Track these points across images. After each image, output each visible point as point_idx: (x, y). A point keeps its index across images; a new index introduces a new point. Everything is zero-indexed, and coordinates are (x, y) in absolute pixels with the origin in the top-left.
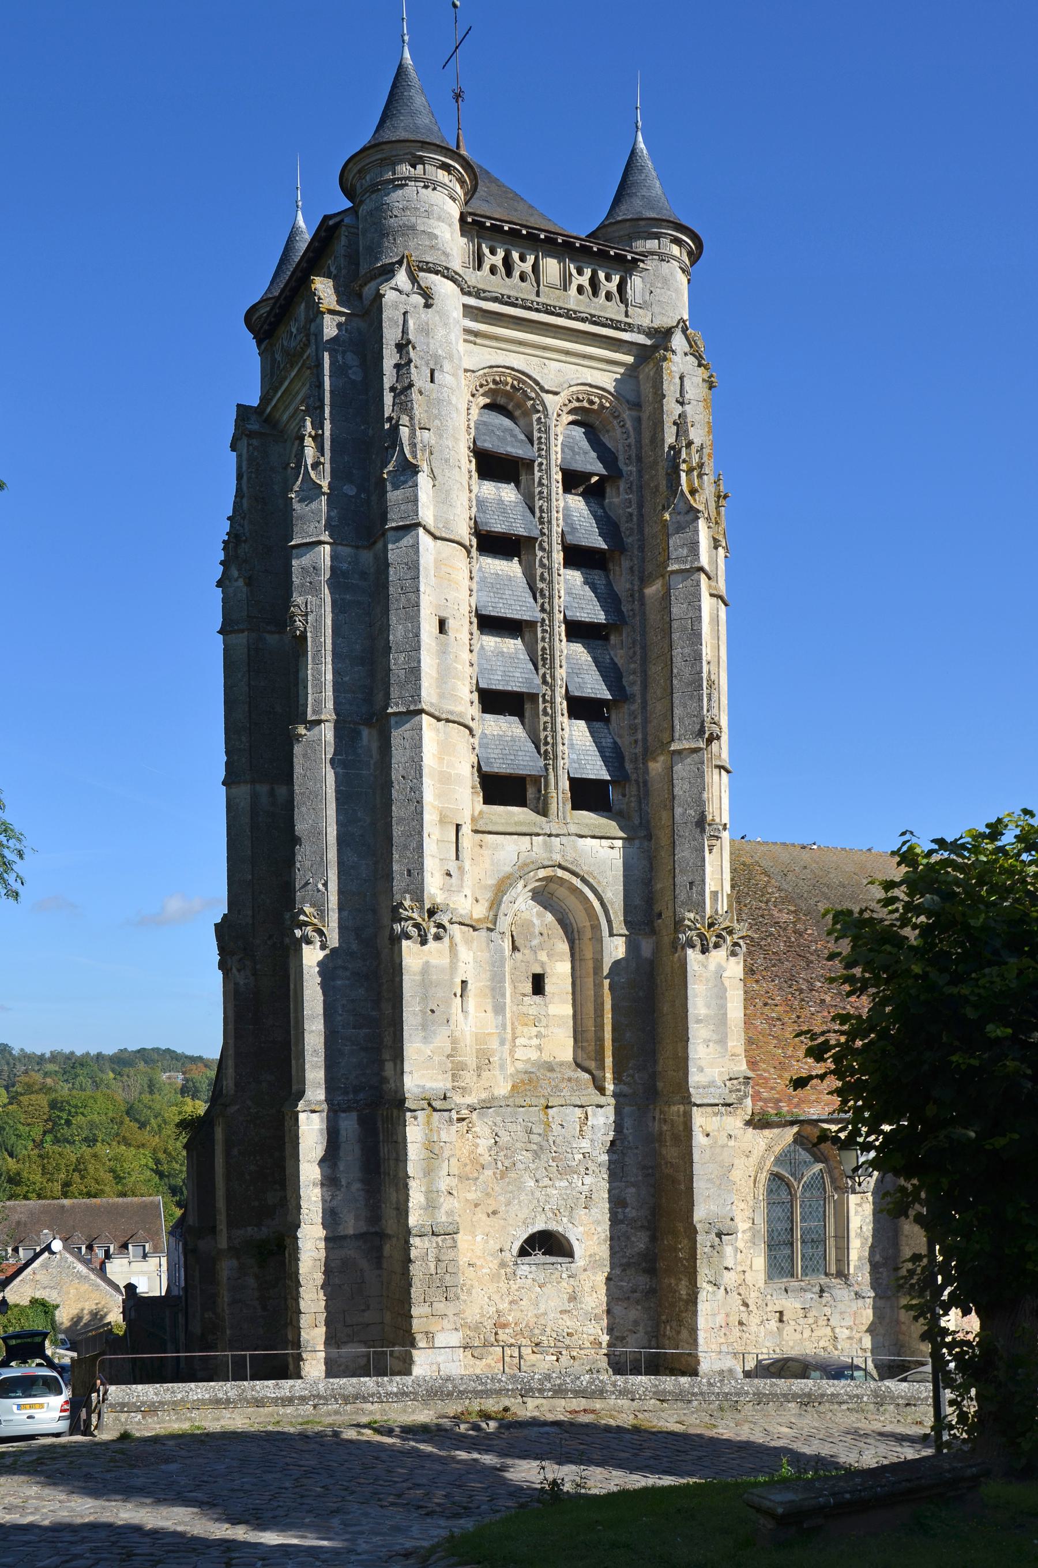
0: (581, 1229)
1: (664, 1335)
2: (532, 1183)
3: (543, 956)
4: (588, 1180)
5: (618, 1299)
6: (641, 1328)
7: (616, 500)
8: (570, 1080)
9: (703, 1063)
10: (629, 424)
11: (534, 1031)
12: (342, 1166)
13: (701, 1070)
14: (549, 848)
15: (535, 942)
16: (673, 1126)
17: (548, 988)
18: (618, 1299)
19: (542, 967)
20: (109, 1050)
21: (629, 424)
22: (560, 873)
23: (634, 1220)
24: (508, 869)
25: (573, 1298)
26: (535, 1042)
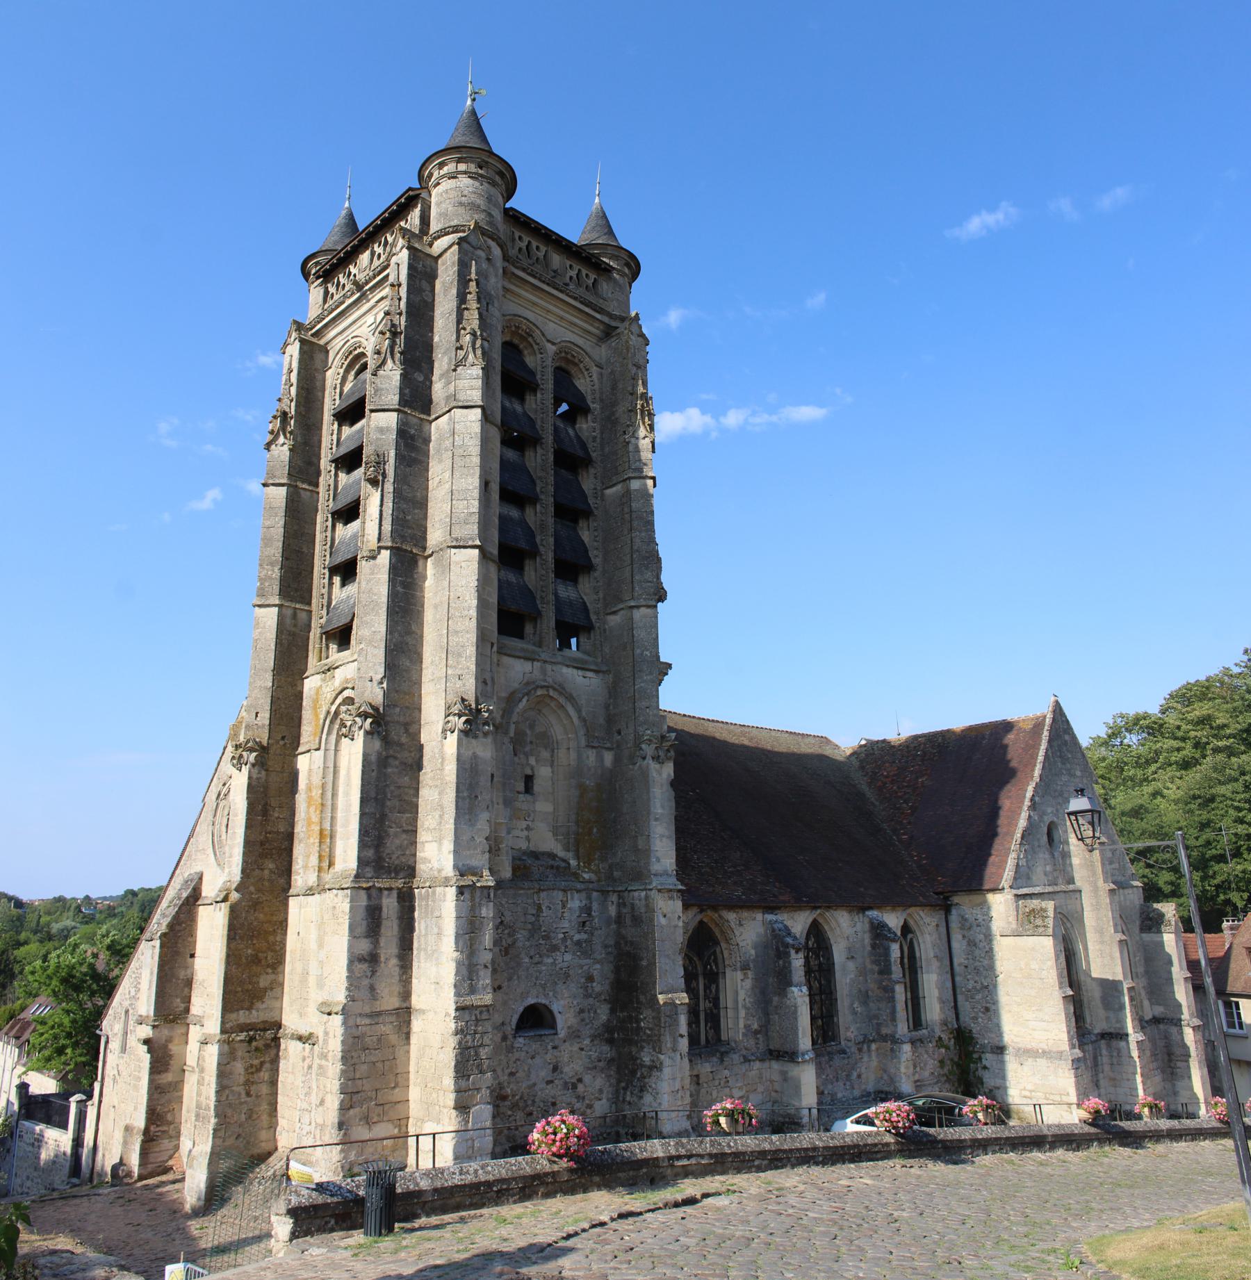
0: (562, 1002)
1: (624, 1100)
2: (527, 960)
3: (532, 761)
4: (568, 957)
5: (589, 1069)
6: (604, 1096)
7: (584, 426)
8: (552, 867)
9: (659, 854)
10: (595, 377)
11: (524, 824)
12: (382, 941)
13: (658, 860)
14: (544, 672)
15: (527, 749)
16: (633, 908)
17: (536, 788)
18: (589, 1069)
19: (532, 769)
20: (665, 579)
21: (595, 377)
22: (552, 693)
23: (600, 994)
24: (516, 685)
25: (555, 1069)
26: (526, 833)
